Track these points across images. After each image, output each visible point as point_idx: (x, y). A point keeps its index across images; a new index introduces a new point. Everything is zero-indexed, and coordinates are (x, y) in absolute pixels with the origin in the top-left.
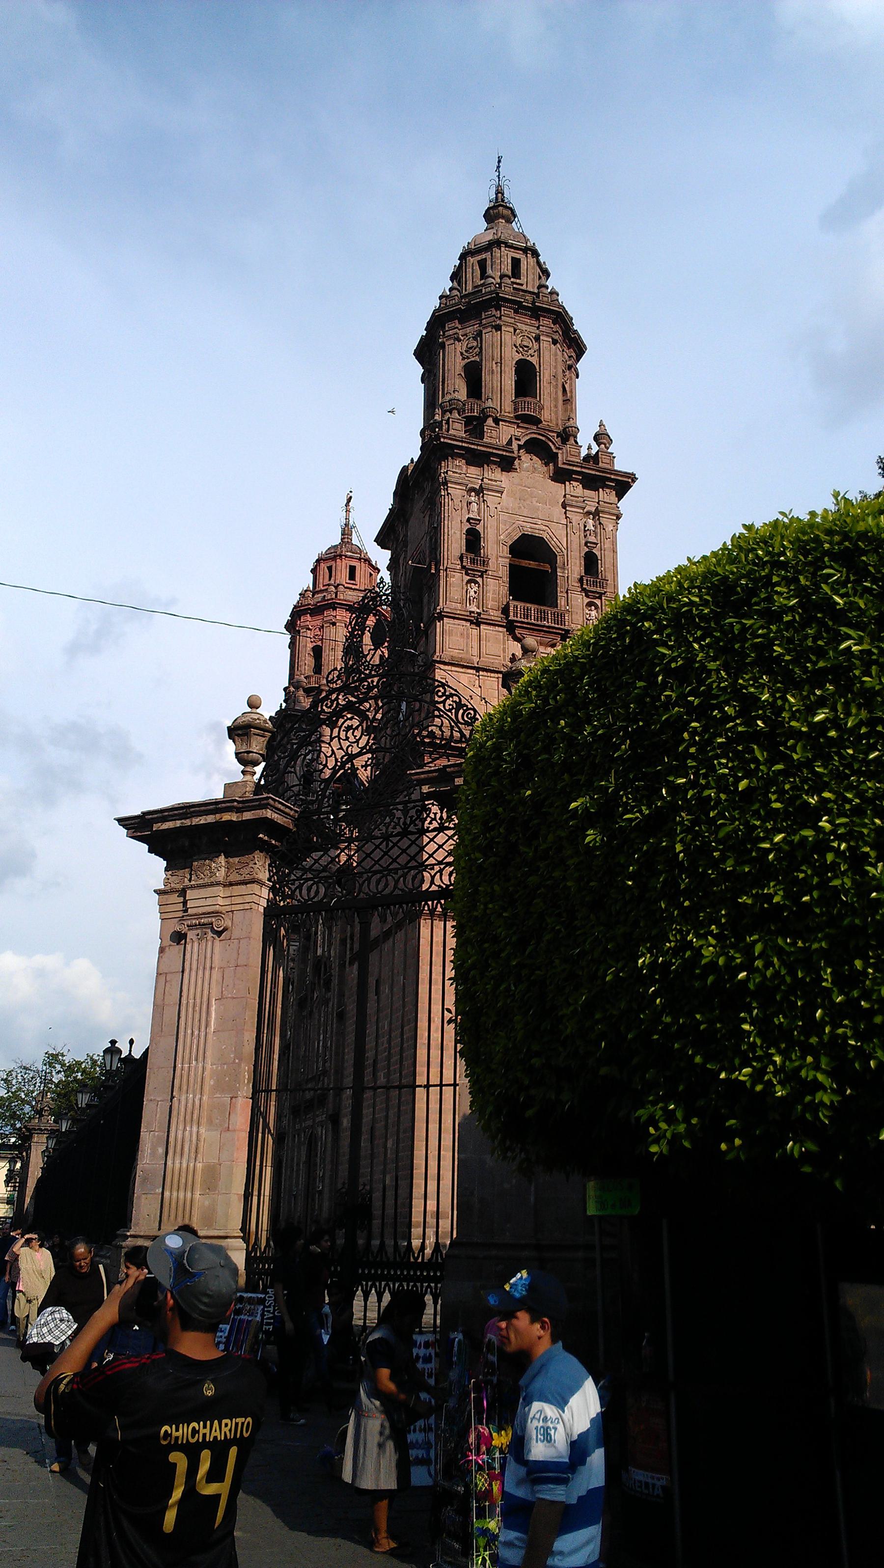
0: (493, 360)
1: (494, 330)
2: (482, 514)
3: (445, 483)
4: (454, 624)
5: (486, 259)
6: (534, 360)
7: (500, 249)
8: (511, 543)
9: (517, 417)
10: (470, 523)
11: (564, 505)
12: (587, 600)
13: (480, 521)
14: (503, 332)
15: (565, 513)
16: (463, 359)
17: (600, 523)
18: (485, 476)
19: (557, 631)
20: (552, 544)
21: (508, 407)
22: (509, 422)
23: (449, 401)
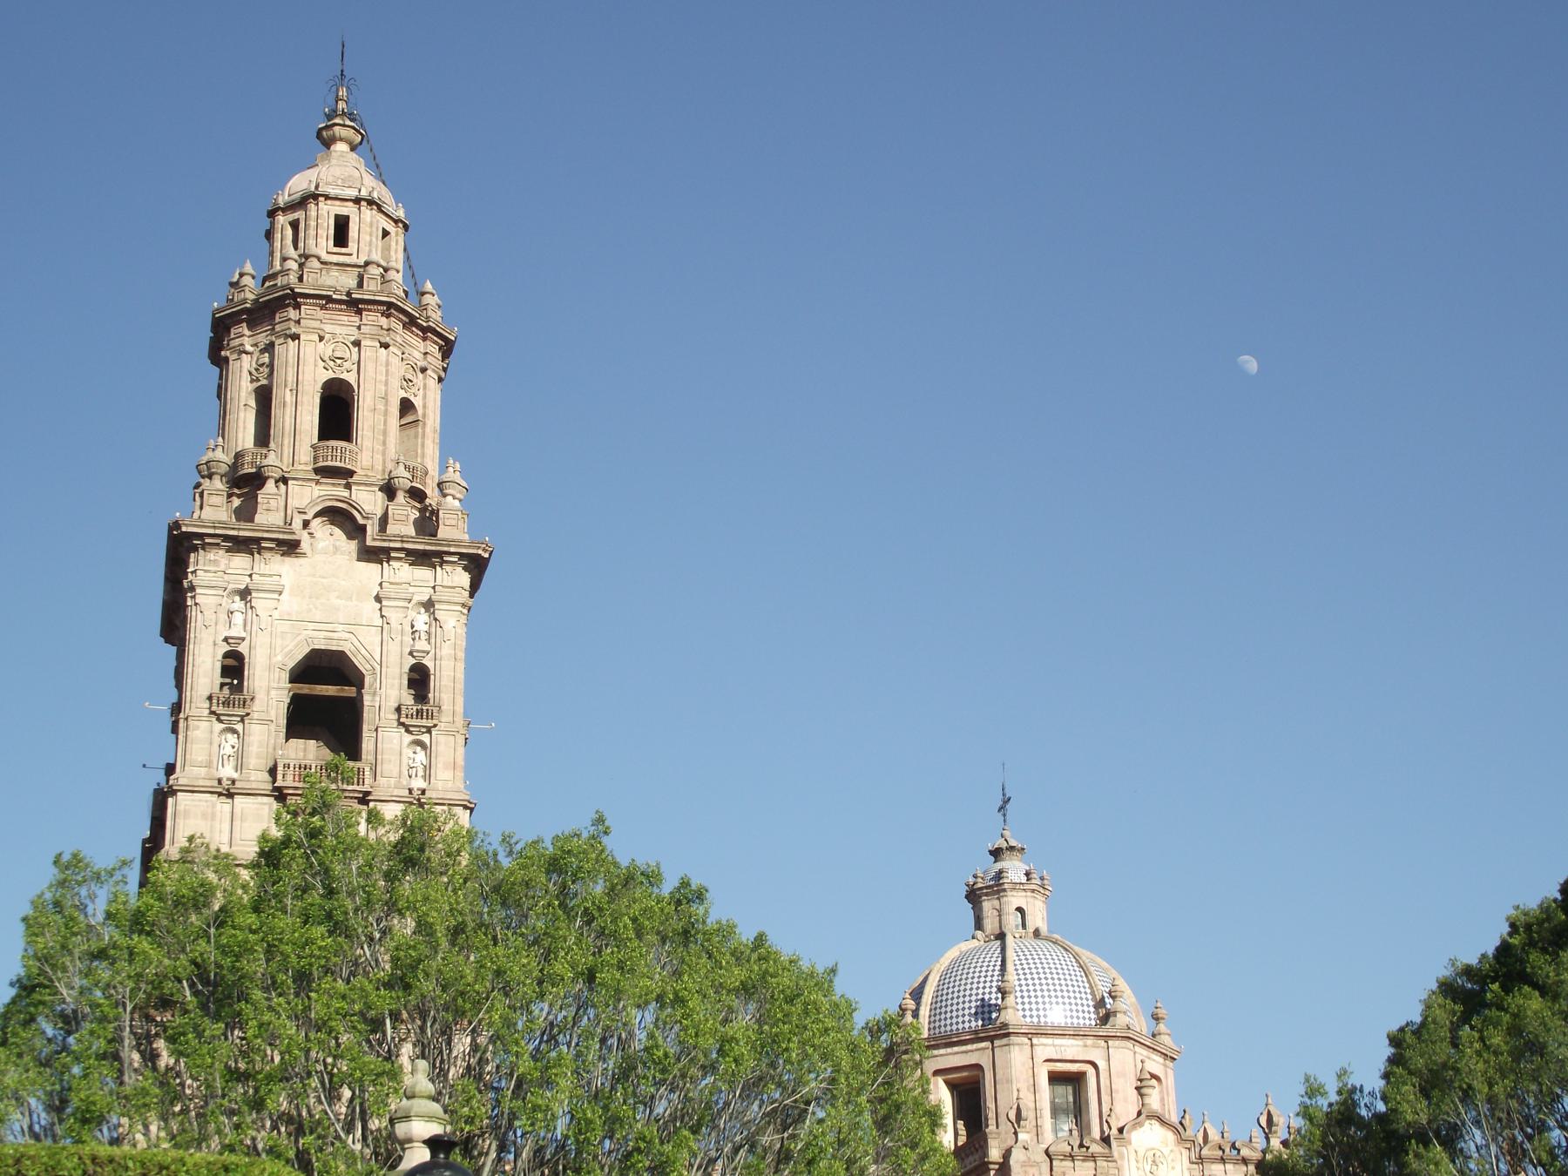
0: (286, 386)
1: (290, 339)
2: (248, 628)
3: (192, 588)
4: (193, 800)
5: (298, 219)
6: (351, 378)
7: (317, 204)
8: (291, 664)
9: (317, 471)
10: (228, 643)
11: (378, 599)
12: (408, 738)
13: (243, 639)
14: (302, 343)
15: (381, 610)
16: (252, 381)
17: (436, 619)
18: (255, 570)
19: (351, 795)
20: (358, 661)
21: (305, 456)
22: (303, 480)
23: (206, 464)
